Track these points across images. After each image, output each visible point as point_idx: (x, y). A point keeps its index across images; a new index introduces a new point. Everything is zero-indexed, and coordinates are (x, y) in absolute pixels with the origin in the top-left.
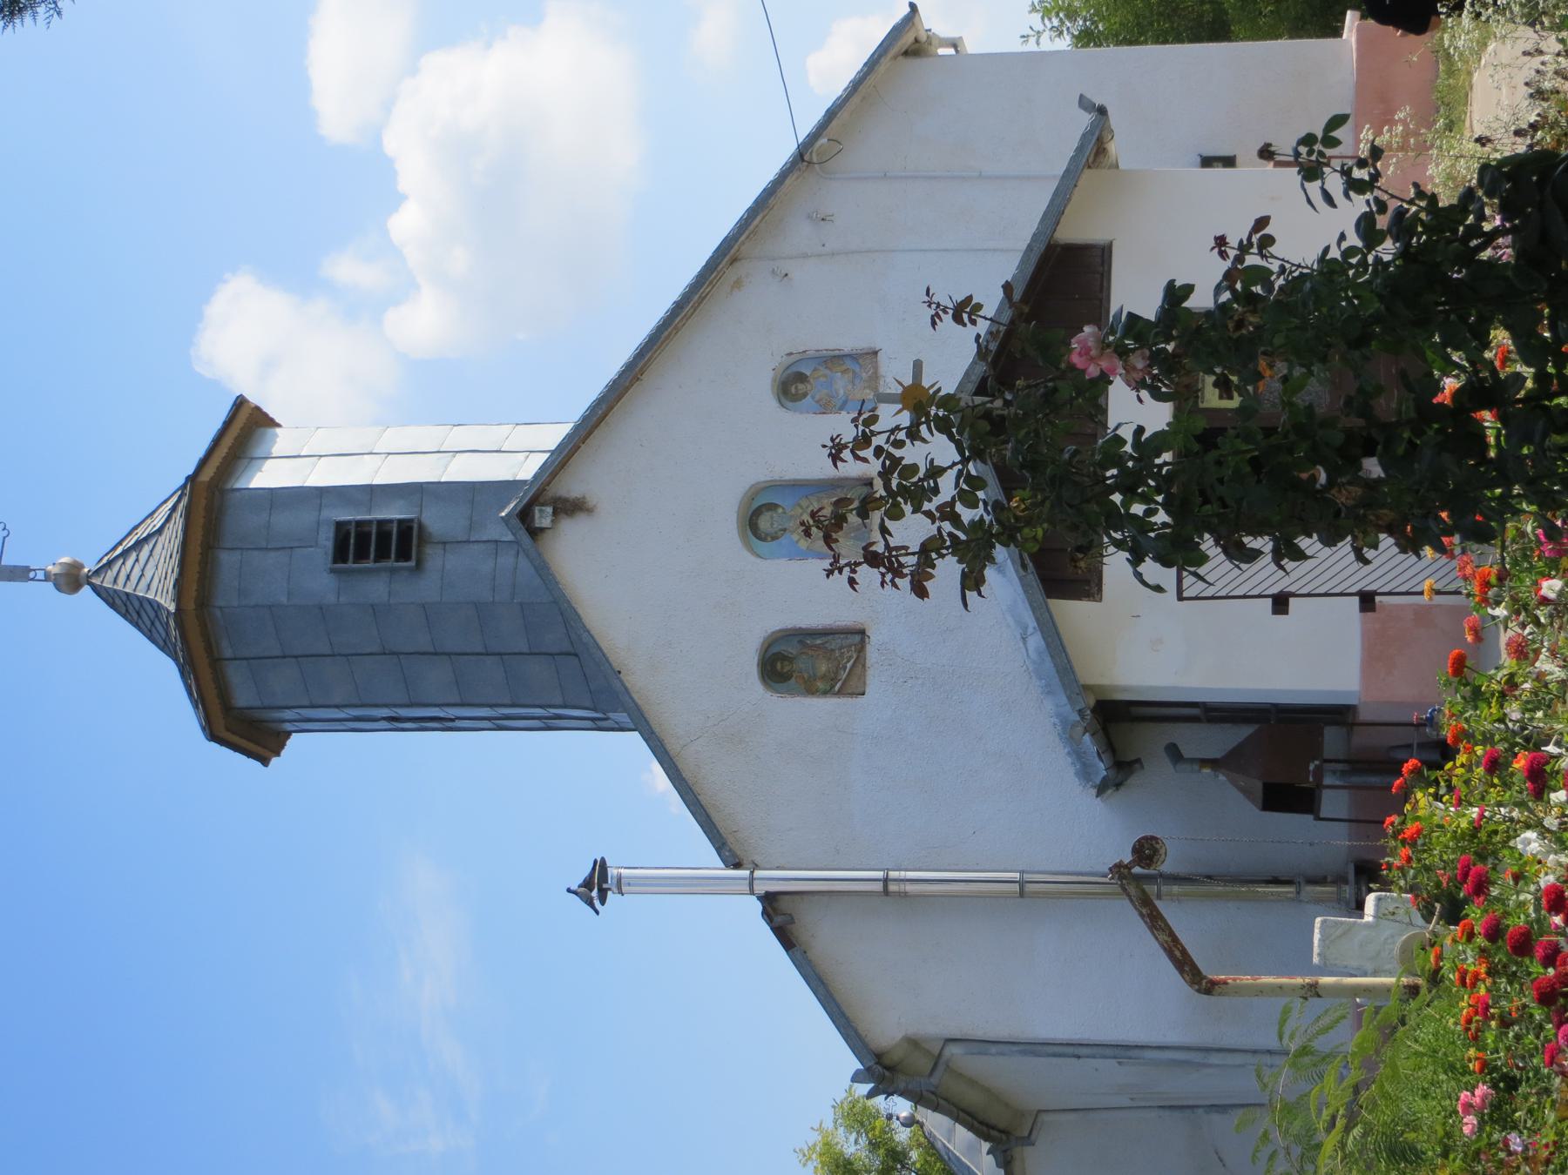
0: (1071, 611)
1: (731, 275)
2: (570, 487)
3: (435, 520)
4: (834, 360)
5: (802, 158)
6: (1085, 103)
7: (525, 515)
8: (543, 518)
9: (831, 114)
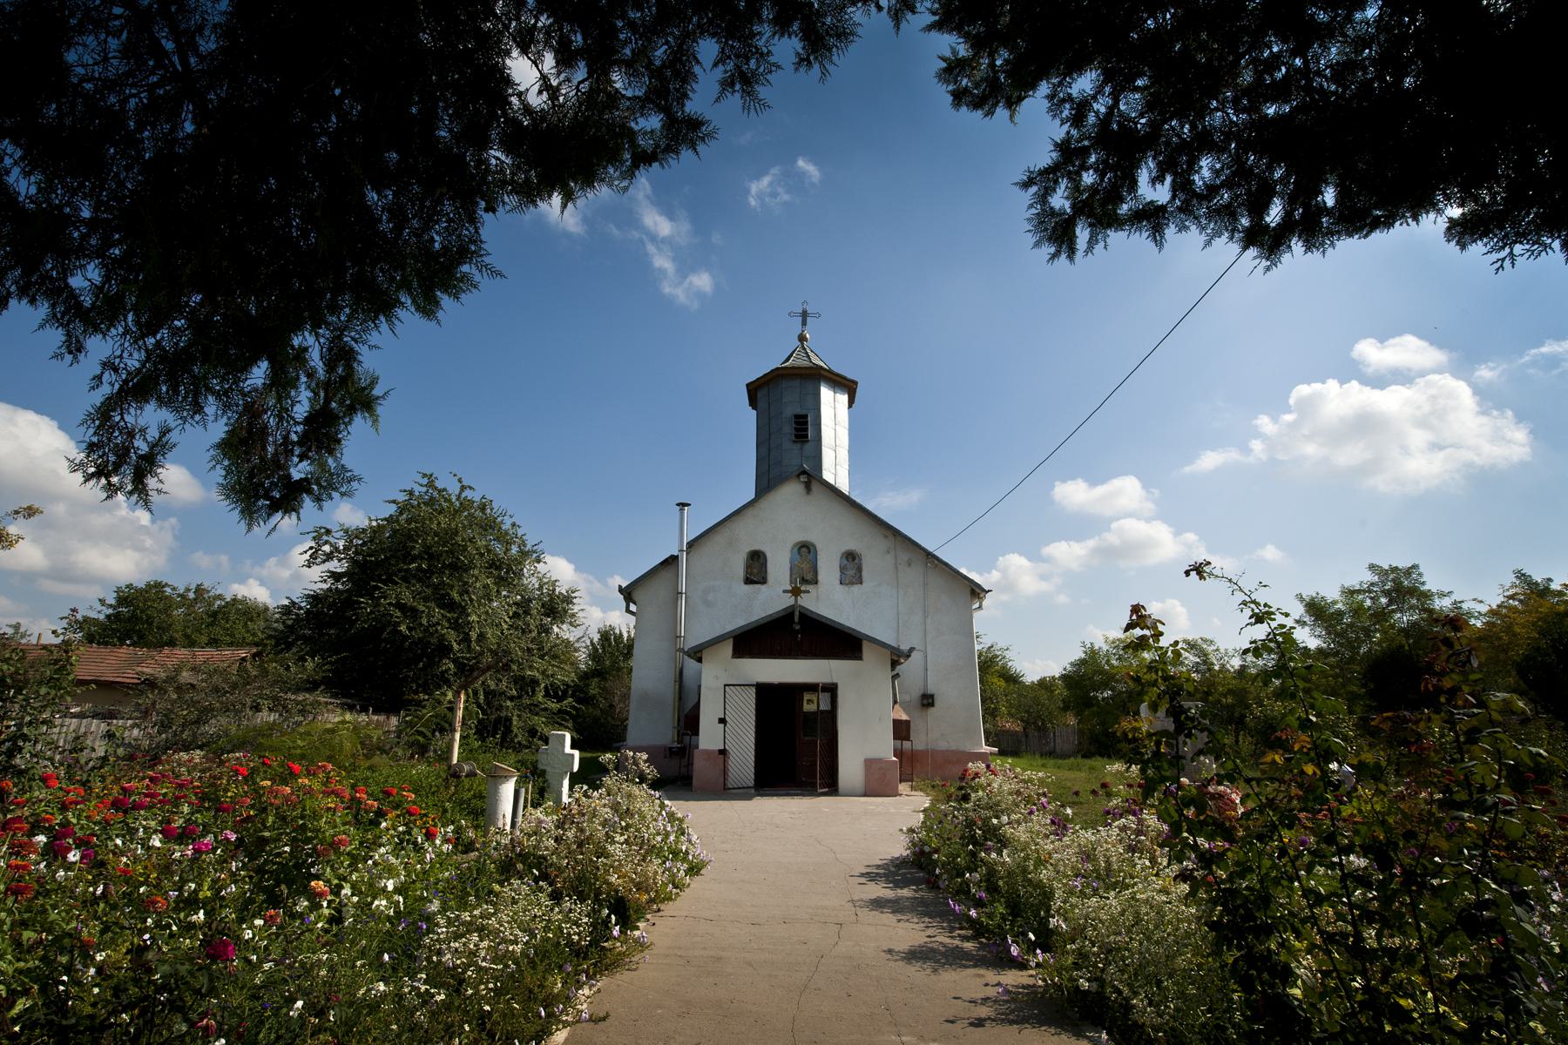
0: (728, 648)
1: (889, 534)
2: (815, 486)
3: (808, 447)
4: (859, 570)
5: (929, 555)
6: (912, 649)
7: (804, 472)
8: (803, 478)
9: (946, 564)
